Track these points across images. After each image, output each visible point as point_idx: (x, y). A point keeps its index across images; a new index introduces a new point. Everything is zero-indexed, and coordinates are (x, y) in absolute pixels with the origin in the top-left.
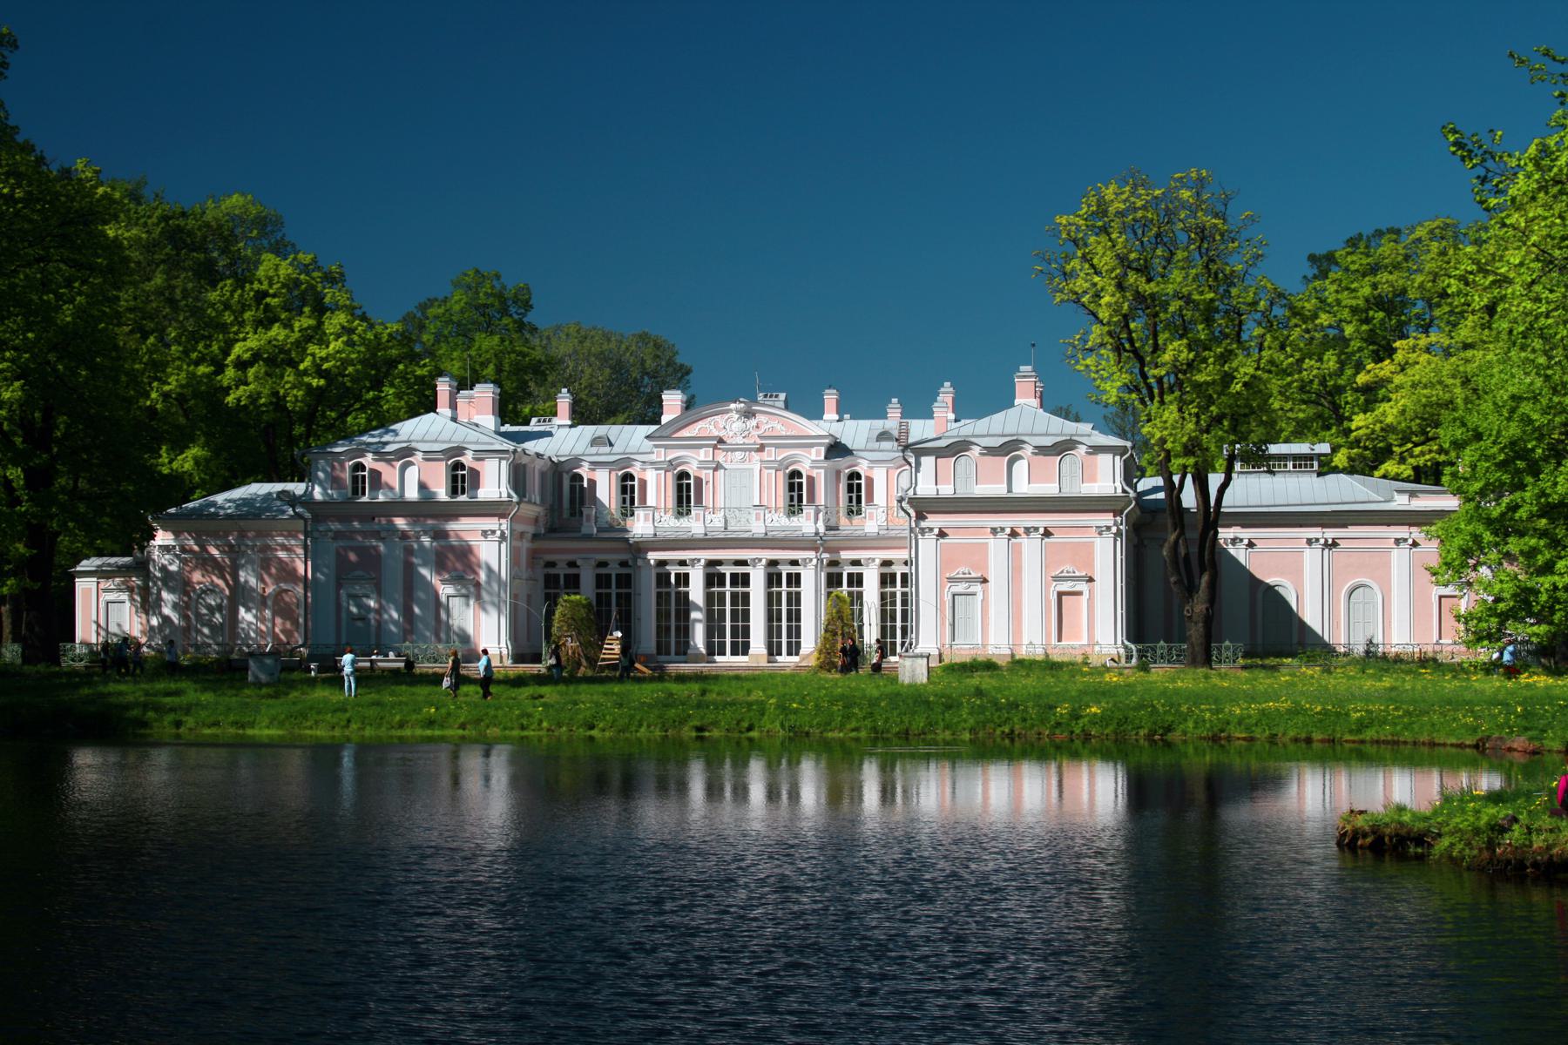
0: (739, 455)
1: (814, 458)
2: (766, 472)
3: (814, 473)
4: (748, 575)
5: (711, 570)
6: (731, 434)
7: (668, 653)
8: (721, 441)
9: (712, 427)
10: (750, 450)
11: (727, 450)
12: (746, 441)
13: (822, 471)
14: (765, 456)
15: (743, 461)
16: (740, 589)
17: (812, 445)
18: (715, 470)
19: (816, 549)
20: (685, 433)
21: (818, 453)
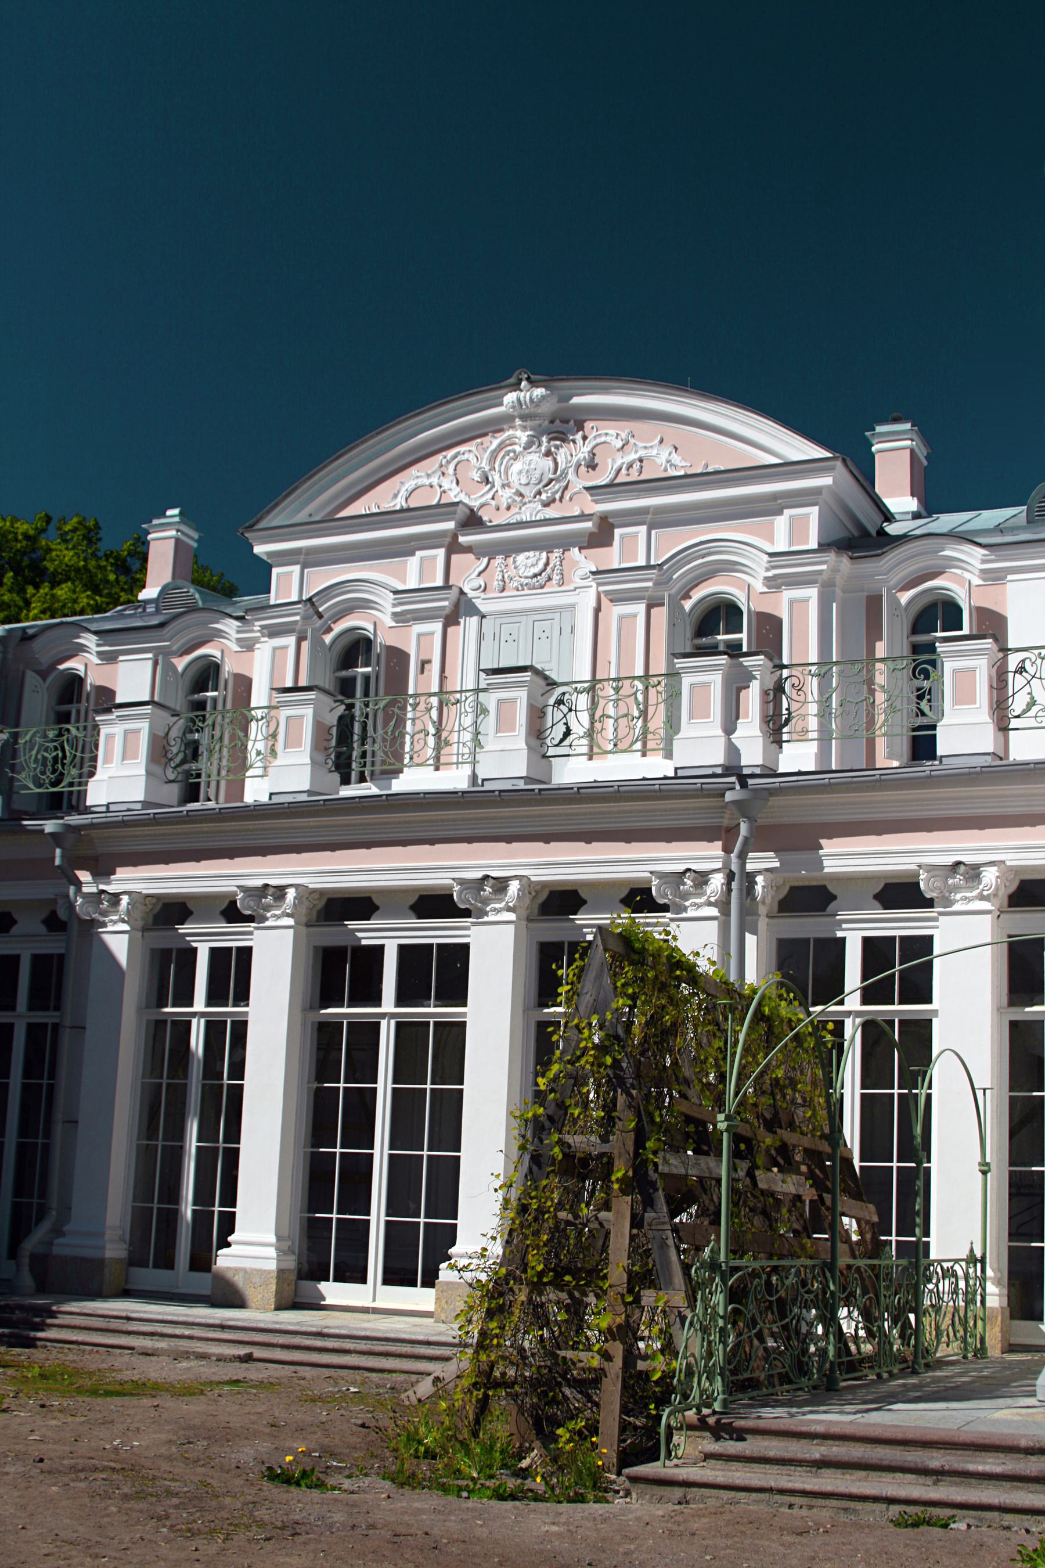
0: (528, 562)
1: (781, 546)
2: (614, 612)
3: (781, 605)
4: (462, 951)
5: (330, 936)
6: (505, 495)
7: (166, 1261)
8: (472, 521)
9: (448, 483)
10: (565, 543)
11: (490, 551)
12: (551, 513)
13: (812, 593)
14: (612, 557)
15: (540, 581)
16: (432, 1011)
17: (772, 506)
18: (451, 620)
19: (726, 835)
20: (358, 508)
21: (796, 529)
